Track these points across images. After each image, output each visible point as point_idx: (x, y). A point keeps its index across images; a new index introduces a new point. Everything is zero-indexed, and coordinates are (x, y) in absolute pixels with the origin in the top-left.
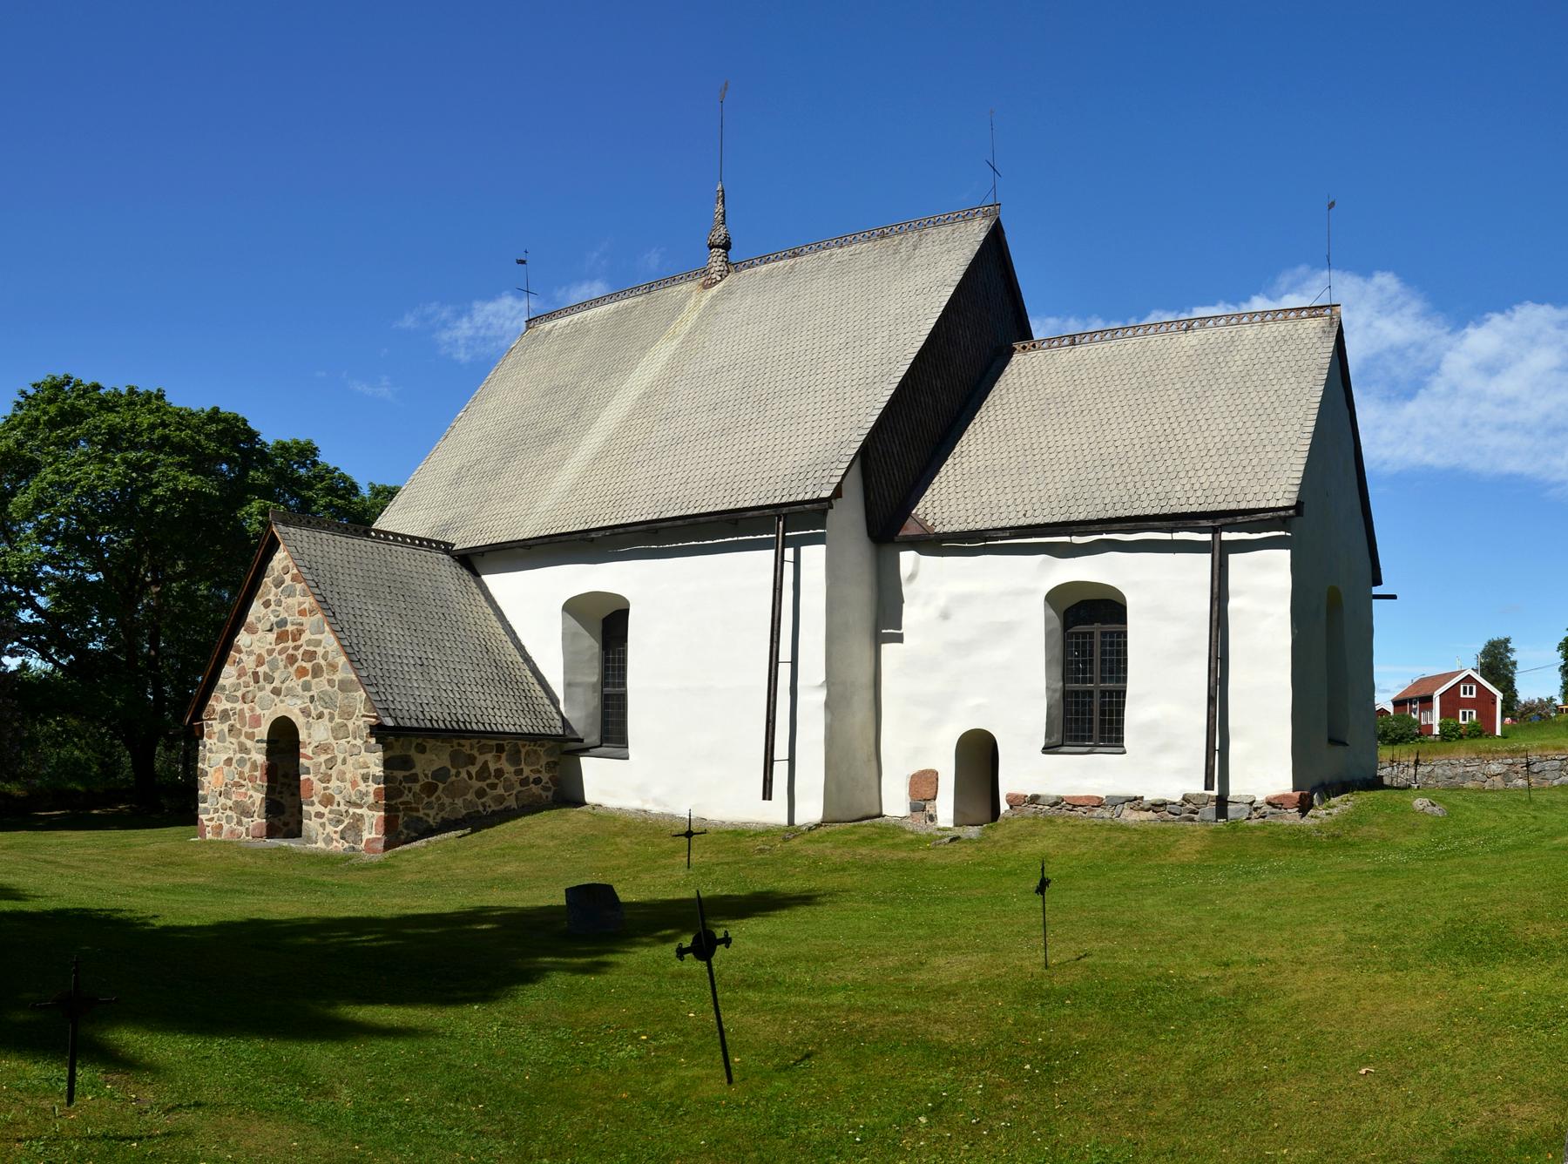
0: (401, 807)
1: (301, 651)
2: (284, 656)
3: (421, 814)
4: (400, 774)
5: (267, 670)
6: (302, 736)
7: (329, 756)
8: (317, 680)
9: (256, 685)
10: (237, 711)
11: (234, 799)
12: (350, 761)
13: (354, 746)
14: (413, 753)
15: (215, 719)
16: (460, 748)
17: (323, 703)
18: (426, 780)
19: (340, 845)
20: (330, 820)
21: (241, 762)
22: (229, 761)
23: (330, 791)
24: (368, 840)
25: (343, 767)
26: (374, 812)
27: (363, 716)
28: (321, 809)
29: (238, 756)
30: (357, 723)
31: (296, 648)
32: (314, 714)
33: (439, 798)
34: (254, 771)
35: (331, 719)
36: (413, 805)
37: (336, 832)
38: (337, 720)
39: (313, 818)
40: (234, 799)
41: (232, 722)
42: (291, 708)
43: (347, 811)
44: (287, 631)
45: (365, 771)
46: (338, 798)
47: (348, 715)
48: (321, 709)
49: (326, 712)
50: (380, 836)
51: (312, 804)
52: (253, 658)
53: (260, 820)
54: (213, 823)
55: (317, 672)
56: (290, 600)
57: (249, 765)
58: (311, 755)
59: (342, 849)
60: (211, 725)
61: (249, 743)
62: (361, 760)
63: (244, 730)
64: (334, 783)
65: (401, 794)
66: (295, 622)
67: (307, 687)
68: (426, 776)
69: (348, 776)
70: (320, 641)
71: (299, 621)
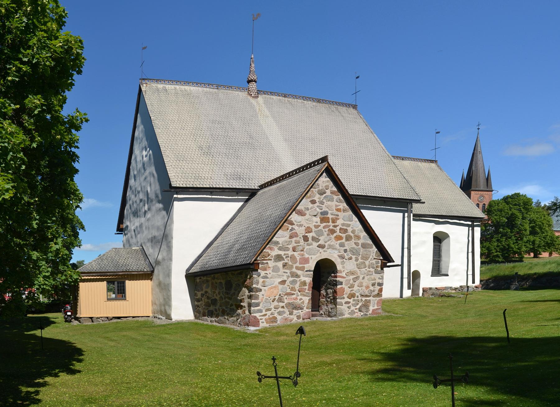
1: (338, 228)
2: (327, 229)
5: (315, 235)
6: (339, 267)
7: (355, 276)
8: (348, 242)
9: (306, 243)
10: (290, 256)
11: (286, 301)
12: (366, 278)
13: (369, 271)
15: (271, 260)
17: (352, 253)
19: (359, 314)
20: (352, 304)
21: (294, 282)
22: (283, 282)
23: (353, 292)
24: (373, 310)
25: (362, 281)
26: (376, 298)
27: (374, 259)
28: (349, 300)
29: (291, 279)
30: (371, 262)
31: (335, 226)
32: (347, 257)
34: (304, 286)
35: (357, 260)
37: (356, 309)
38: (360, 260)
39: (344, 304)
40: (286, 301)
41: (286, 261)
42: (333, 255)
43: (361, 300)
44: (329, 218)
45: (374, 281)
46: (357, 294)
47: (365, 258)
48: (351, 255)
49: (354, 257)
50: (380, 307)
51: (344, 298)
52: (303, 228)
53: (308, 310)
54: (267, 317)
55: (348, 238)
56: (329, 203)
57: (298, 283)
58: (345, 276)
59: (360, 315)
60: (267, 263)
61: (299, 272)
62: (372, 277)
63: (294, 266)
64: (356, 288)
66: (334, 214)
67: (342, 245)
69: (364, 284)
70: (350, 225)
71: (336, 214)
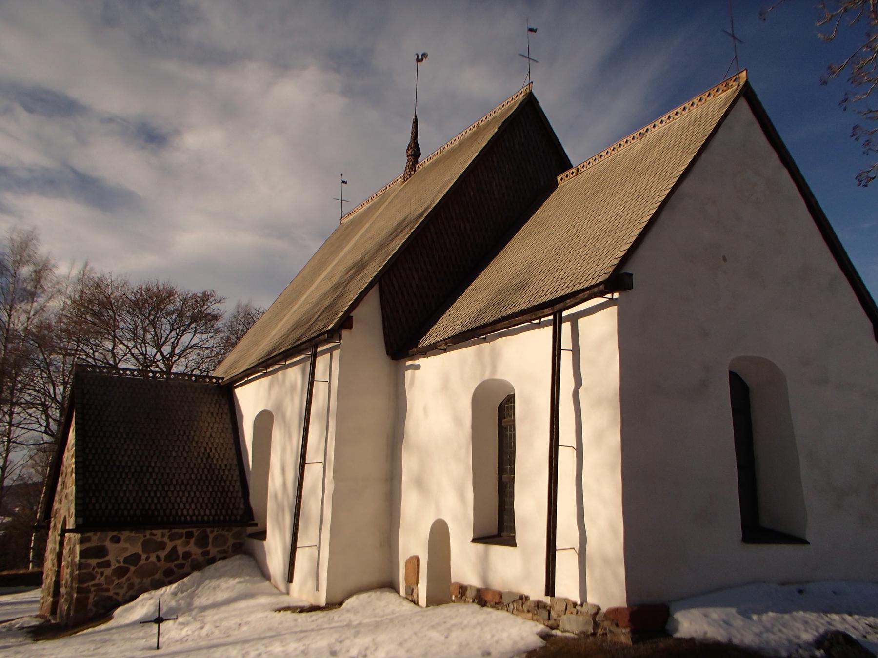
0: (93, 589)
3: (111, 593)
4: (93, 562)
14: (108, 544)
16: (153, 537)
18: (117, 565)
33: (128, 579)
36: (105, 586)
65: (93, 578)
68: (118, 562)
